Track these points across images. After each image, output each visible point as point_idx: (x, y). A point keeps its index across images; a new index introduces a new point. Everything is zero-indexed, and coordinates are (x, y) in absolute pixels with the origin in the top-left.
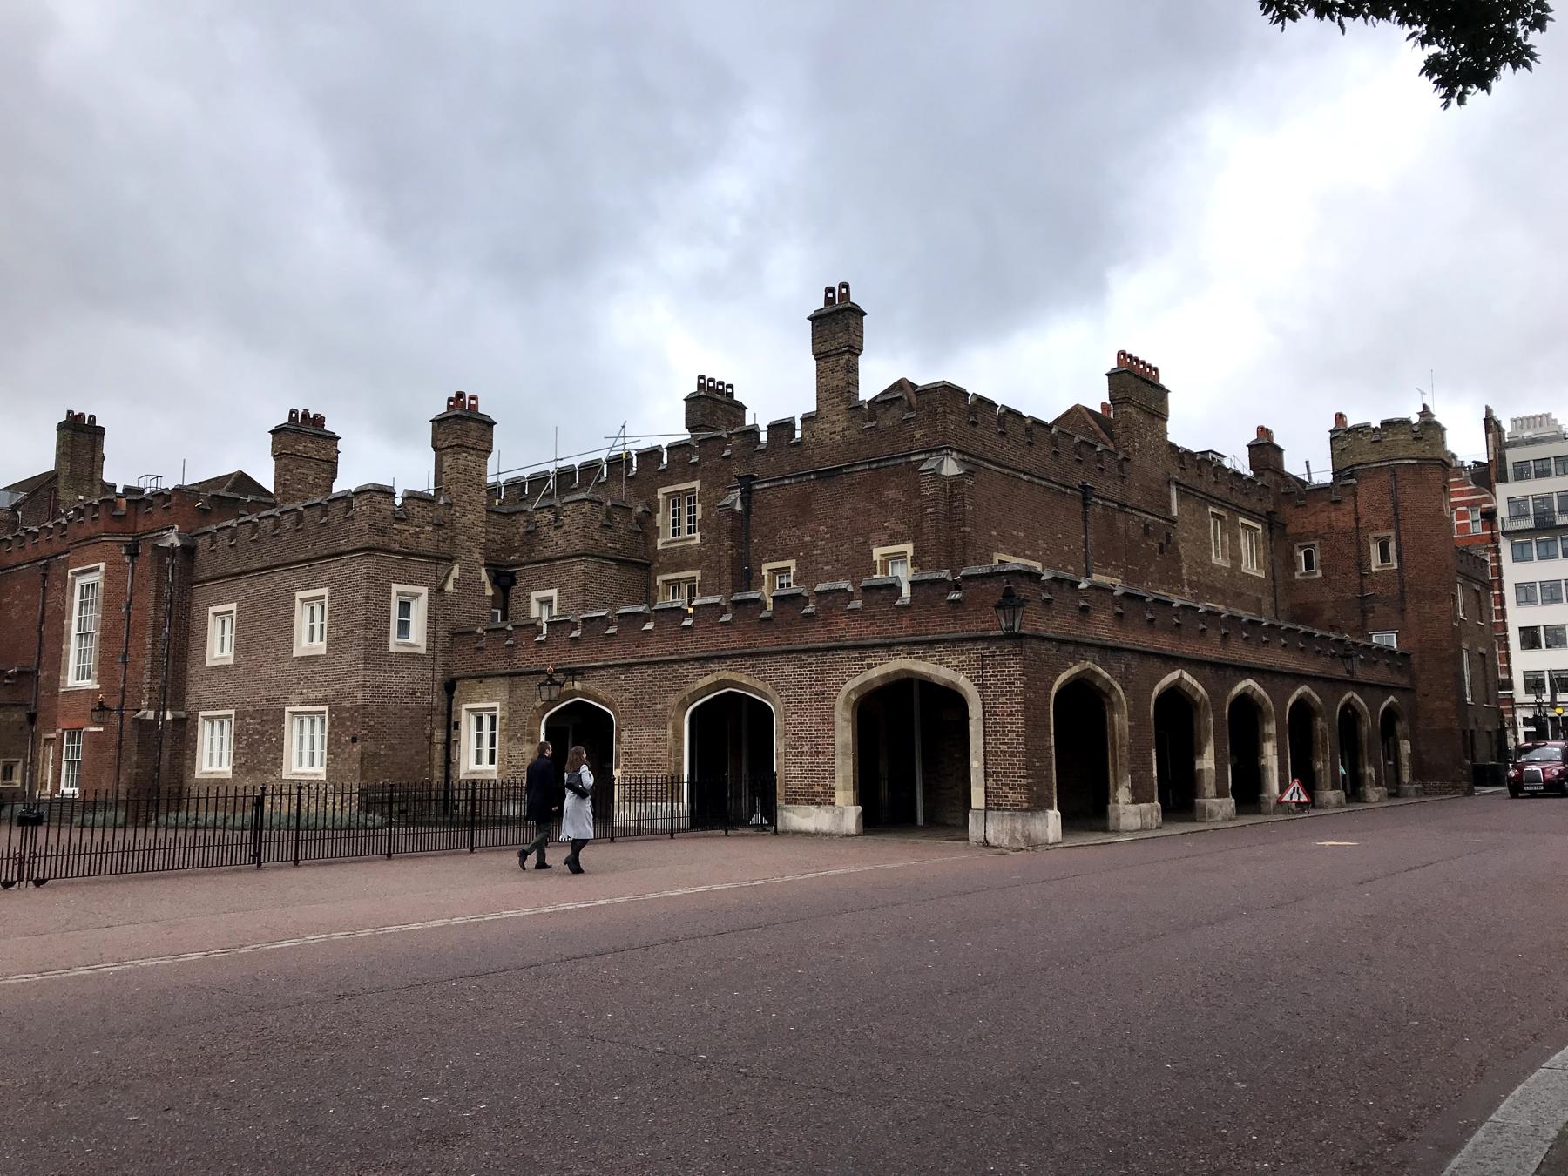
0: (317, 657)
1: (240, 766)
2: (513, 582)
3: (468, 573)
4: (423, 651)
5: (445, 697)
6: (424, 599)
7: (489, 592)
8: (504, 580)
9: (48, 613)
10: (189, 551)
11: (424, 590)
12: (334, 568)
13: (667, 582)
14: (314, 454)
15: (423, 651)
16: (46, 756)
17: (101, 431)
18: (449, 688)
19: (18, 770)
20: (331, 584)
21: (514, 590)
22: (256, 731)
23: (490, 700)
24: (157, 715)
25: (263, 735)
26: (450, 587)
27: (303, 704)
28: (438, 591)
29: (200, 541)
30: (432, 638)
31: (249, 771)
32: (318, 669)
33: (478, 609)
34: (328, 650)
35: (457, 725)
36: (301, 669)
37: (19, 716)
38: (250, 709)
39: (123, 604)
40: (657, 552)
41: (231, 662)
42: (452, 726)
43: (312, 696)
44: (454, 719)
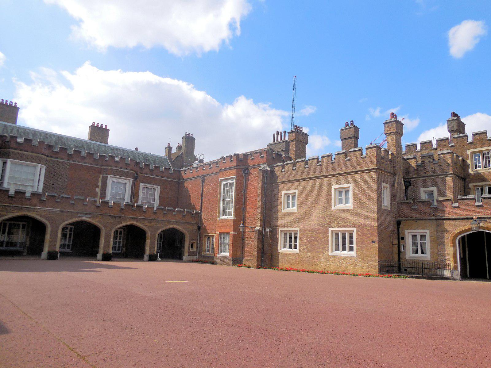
0: (347, 211)
1: (304, 249)
2: (410, 184)
3: (399, 180)
4: (389, 209)
5: (396, 227)
6: (389, 189)
7: (404, 188)
8: (408, 184)
9: (204, 193)
10: (272, 172)
11: (388, 186)
12: (356, 177)
13: (475, 186)
14: (302, 140)
15: (389, 209)
16: (205, 241)
17: (194, 139)
18: (399, 223)
19: (195, 245)
20: (354, 182)
21: (410, 188)
22: (311, 237)
23: (422, 229)
24: (262, 229)
25: (316, 238)
26: (396, 185)
27: (340, 227)
28: (393, 186)
29: (276, 168)
30: (391, 204)
31: (308, 251)
32: (348, 214)
33: (401, 194)
34: (354, 207)
35: (403, 238)
36: (338, 214)
37: (196, 228)
38: (308, 228)
39: (243, 190)
40: (469, 175)
41: (296, 211)
42: (401, 238)
43: (345, 225)
44: (401, 236)
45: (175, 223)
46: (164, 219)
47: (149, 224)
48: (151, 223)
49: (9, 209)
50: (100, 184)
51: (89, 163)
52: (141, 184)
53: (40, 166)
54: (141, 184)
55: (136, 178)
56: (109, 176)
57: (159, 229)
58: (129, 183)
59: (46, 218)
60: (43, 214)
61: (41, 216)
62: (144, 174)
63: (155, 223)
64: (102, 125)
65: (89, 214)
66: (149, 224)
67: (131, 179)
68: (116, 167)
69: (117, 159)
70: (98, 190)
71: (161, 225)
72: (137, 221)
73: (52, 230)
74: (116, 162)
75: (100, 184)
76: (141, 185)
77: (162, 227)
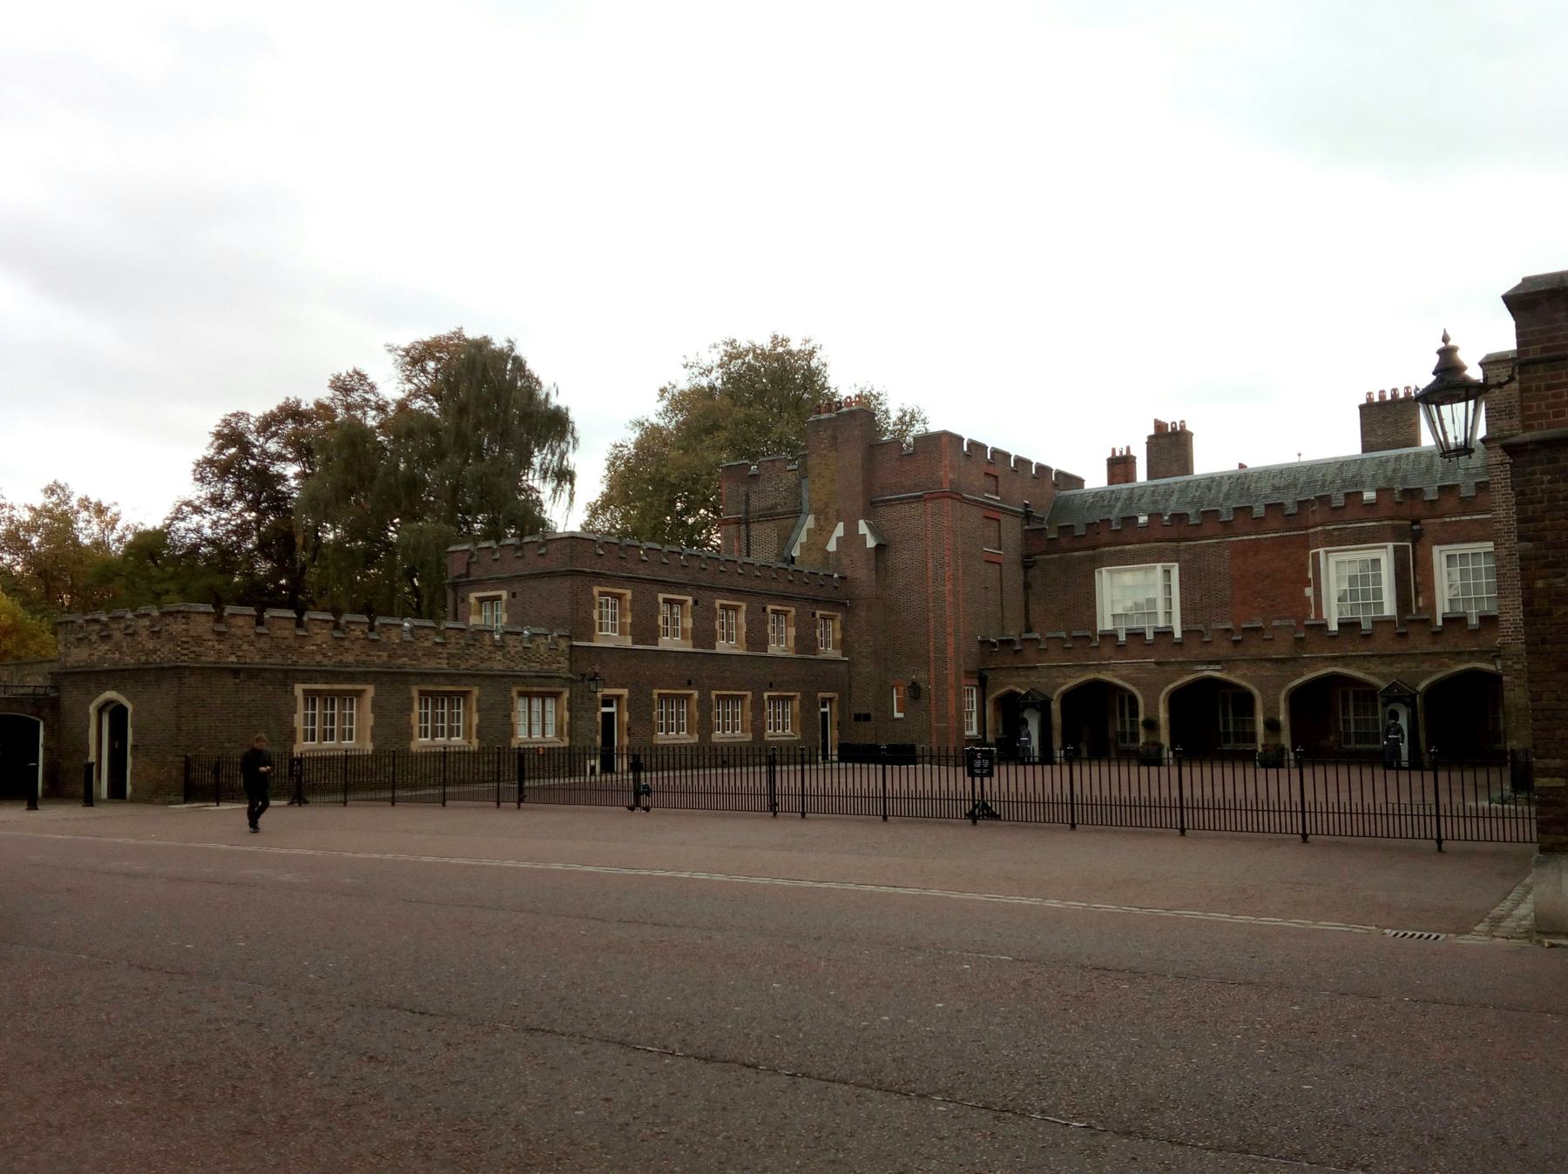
45: (1472, 655)
46: (1438, 648)
47: (1386, 670)
48: (1391, 665)
49: (1066, 671)
50: (1310, 575)
51: (1276, 531)
52: (1436, 549)
53: (1159, 566)
54: (1436, 549)
55: (1417, 538)
56: (1321, 550)
57: (1422, 679)
58: (1385, 556)
59: (1131, 681)
60: (1124, 672)
61: (1123, 678)
62: (1442, 516)
63: (1405, 665)
64: (1394, 390)
65: (1217, 663)
66: (1386, 670)
67: (1390, 545)
68: (1338, 522)
69: (1369, 495)
70: (1309, 591)
71: (1426, 667)
72: (1347, 666)
73: (1146, 705)
74: (1371, 505)
75: (1310, 575)
76: (1439, 554)
77: (1431, 673)
